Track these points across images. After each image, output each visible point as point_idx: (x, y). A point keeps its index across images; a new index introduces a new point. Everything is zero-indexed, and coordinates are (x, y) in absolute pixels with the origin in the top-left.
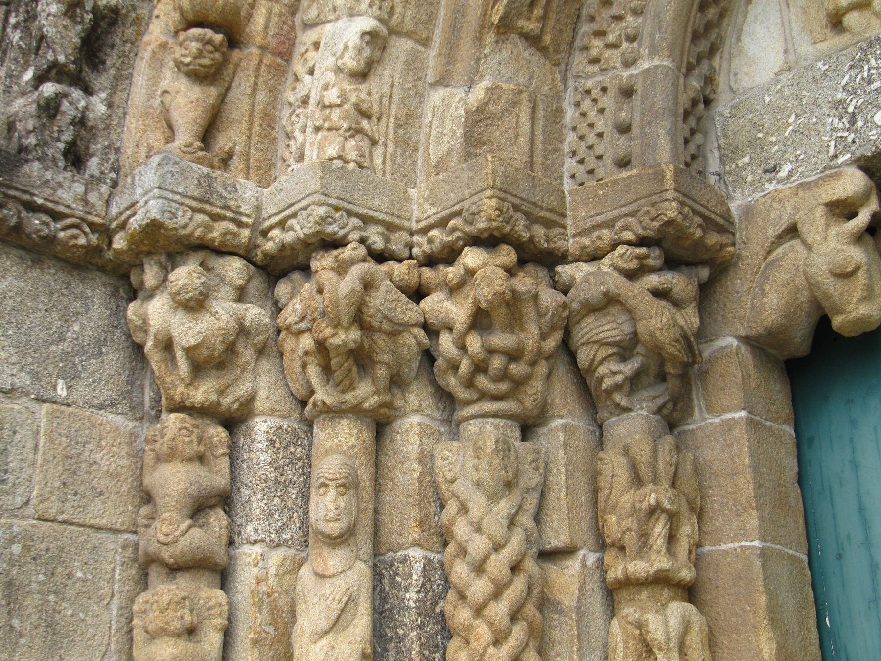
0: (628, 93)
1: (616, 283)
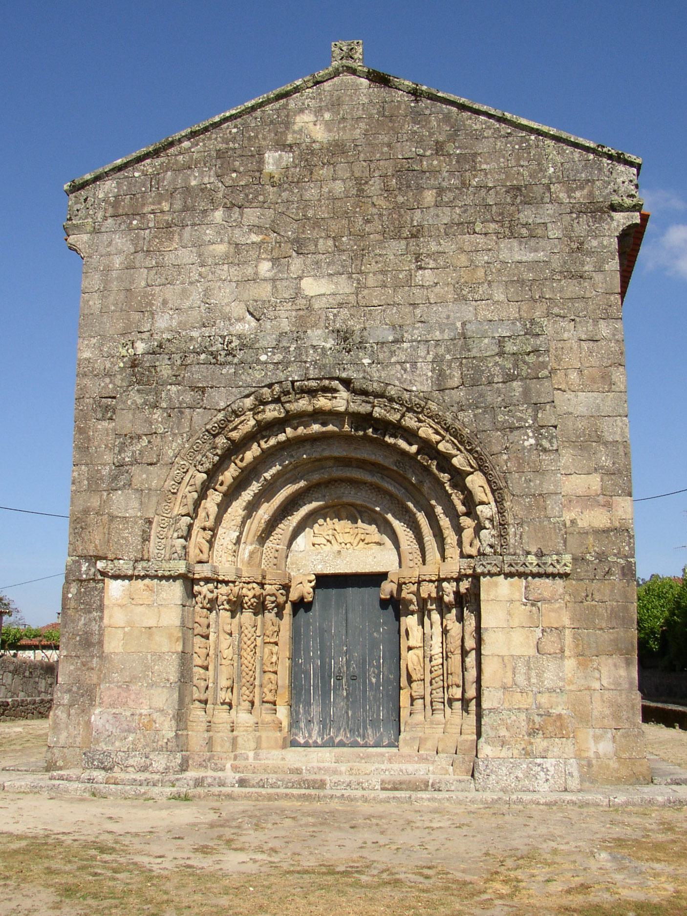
0: (277, 551)
1: (275, 592)
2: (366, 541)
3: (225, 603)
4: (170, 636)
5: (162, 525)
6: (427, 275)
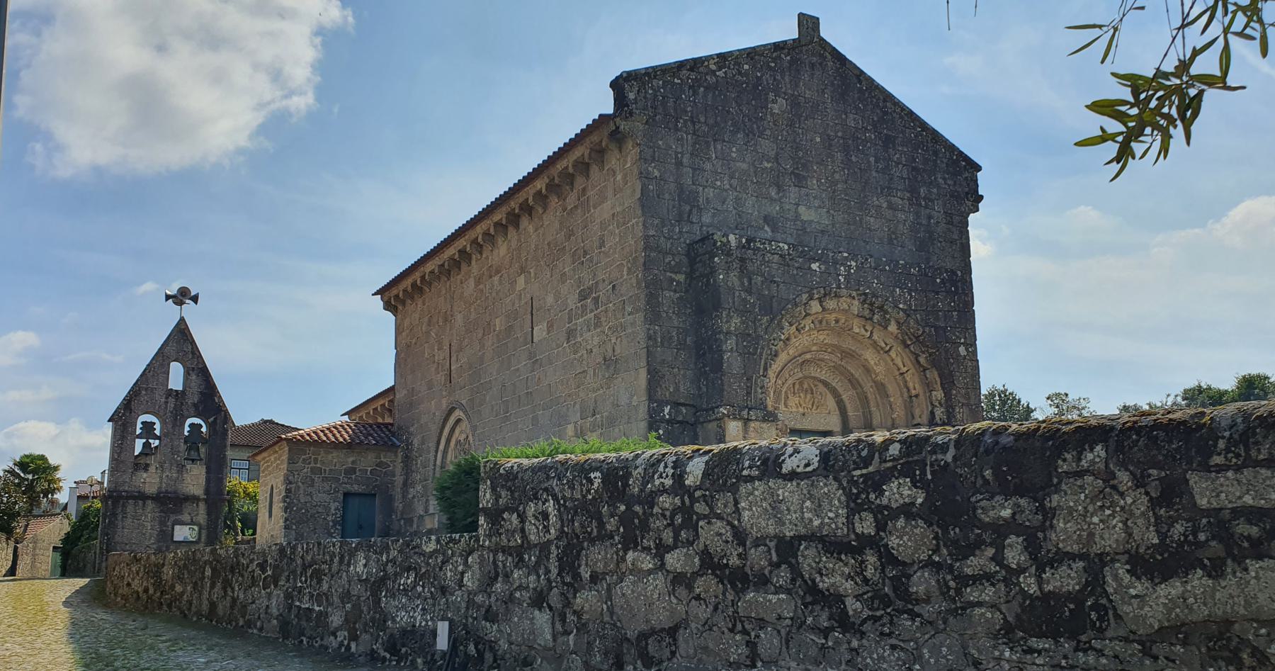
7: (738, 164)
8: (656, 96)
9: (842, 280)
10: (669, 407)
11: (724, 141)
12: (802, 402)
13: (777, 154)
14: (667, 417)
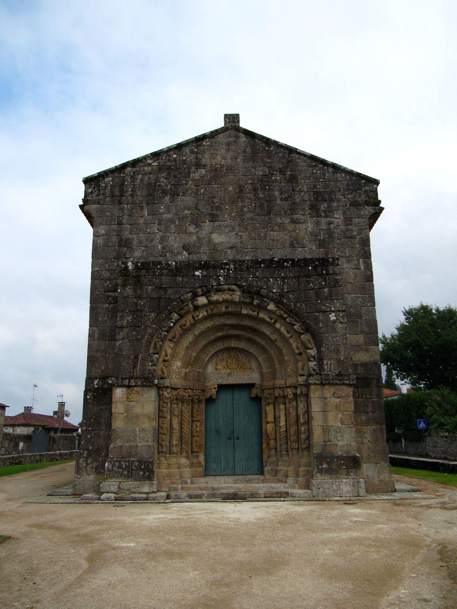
1: (199, 394)
2: (244, 368)
3: (174, 400)
4: (149, 418)
5: (144, 359)
6: (275, 234)
7: (164, 216)
8: (106, 187)
9: (222, 279)
10: (98, 380)
11: (155, 203)
12: (229, 366)
13: (197, 203)
14: (96, 386)
